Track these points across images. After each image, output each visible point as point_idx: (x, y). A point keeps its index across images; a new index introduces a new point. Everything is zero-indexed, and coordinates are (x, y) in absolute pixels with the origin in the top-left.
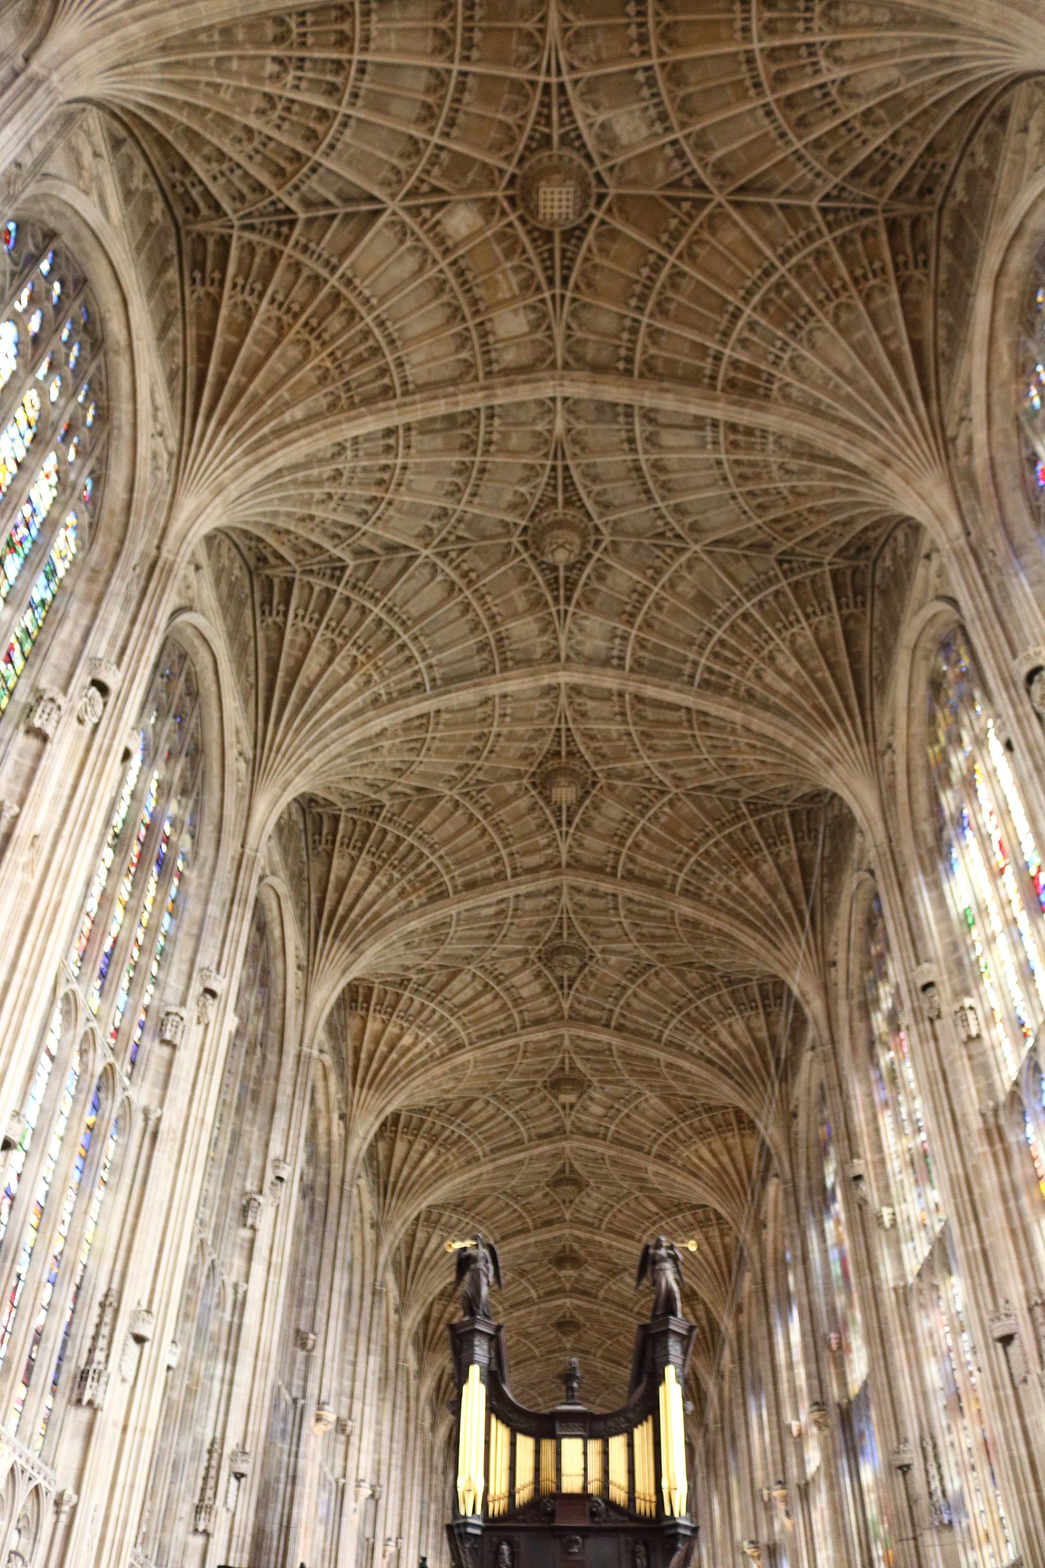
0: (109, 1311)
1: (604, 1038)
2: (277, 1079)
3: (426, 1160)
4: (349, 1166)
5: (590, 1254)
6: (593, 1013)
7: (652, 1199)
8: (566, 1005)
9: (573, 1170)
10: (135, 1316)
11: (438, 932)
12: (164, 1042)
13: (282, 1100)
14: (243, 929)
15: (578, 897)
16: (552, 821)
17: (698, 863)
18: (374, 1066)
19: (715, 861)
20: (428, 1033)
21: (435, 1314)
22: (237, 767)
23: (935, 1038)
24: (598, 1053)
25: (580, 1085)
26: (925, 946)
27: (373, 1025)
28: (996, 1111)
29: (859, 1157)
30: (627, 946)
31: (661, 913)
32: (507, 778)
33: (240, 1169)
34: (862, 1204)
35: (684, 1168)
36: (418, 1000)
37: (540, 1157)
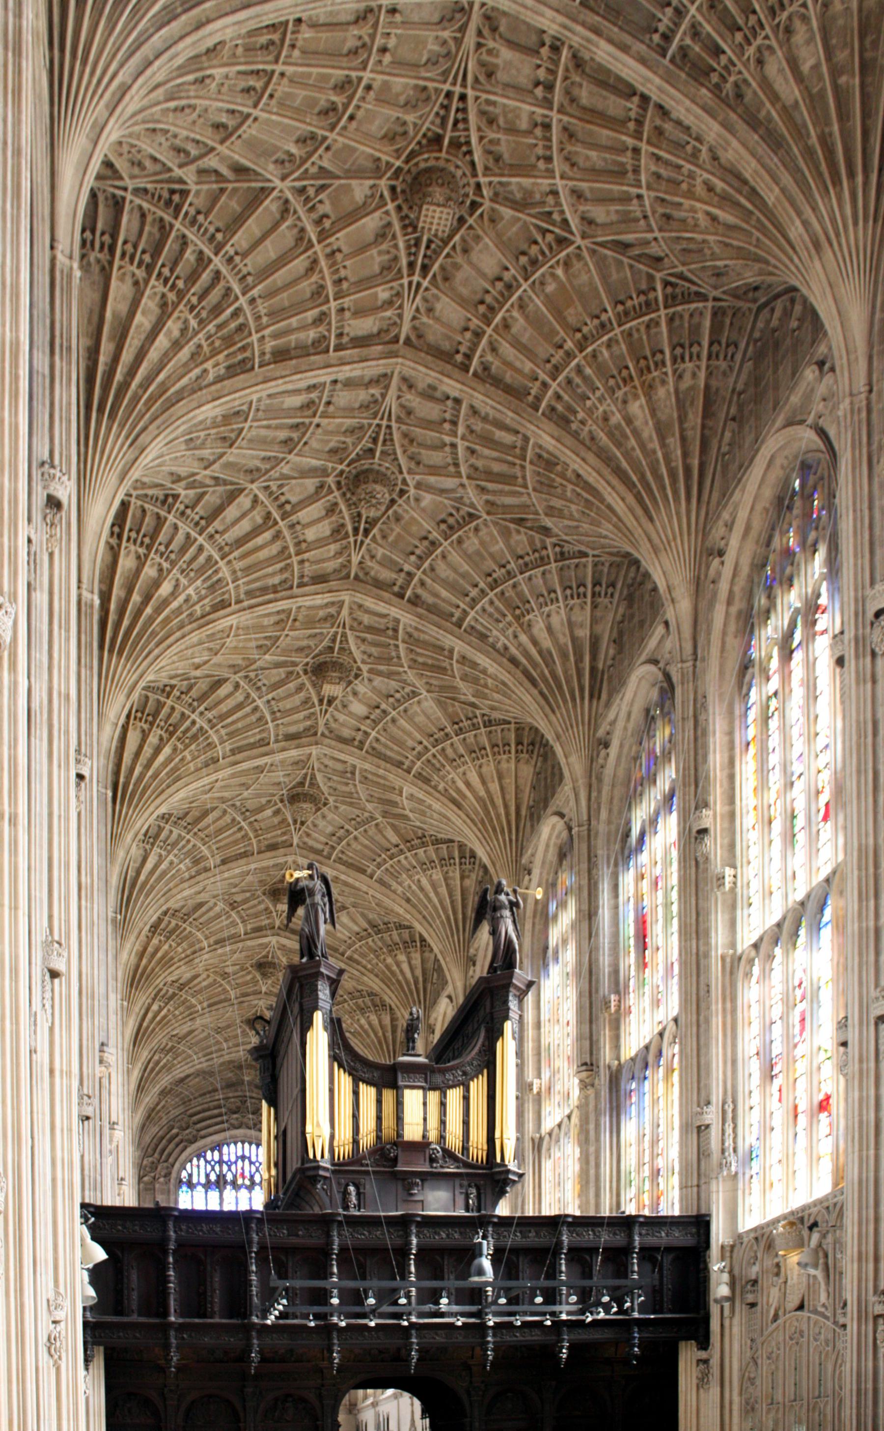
1: (394, 612)
9: (312, 784)
31: (507, 438)
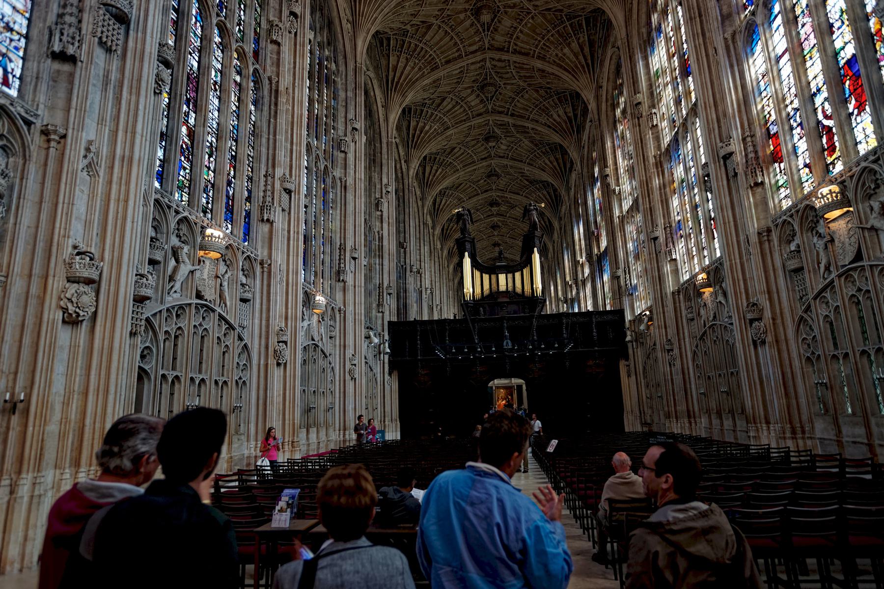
0: (342, 250)
1: (506, 120)
2: (381, 153)
3: (438, 173)
4: (410, 180)
5: (503, 201)
6: (501, 109)
7: (526, 180)
8: (490, 107)
10: (351, 251)
11: (436, 83)
12: (342, 152)
13: (384, 161)
14: (361, 99)
15: (493, 63)
16: (481, 30)
17: (544, 44)
18: (415, 139)
19: (552, 43)
20: (435, 124)
21: (446, 227)
22: (347, 26)
23: (639, 125)
24: (502, 125)
25: (497, 138)
26: (638, 86)
27: (413, 124)
28: (660, 155)
29: (607, 167)
30: (514, 81)
31: (528, 67)
32: (461, 12)
33: (373, 190)
34: (608, 185)
35: (539, 168)
36: (430, 111)
37: (483, 166)
